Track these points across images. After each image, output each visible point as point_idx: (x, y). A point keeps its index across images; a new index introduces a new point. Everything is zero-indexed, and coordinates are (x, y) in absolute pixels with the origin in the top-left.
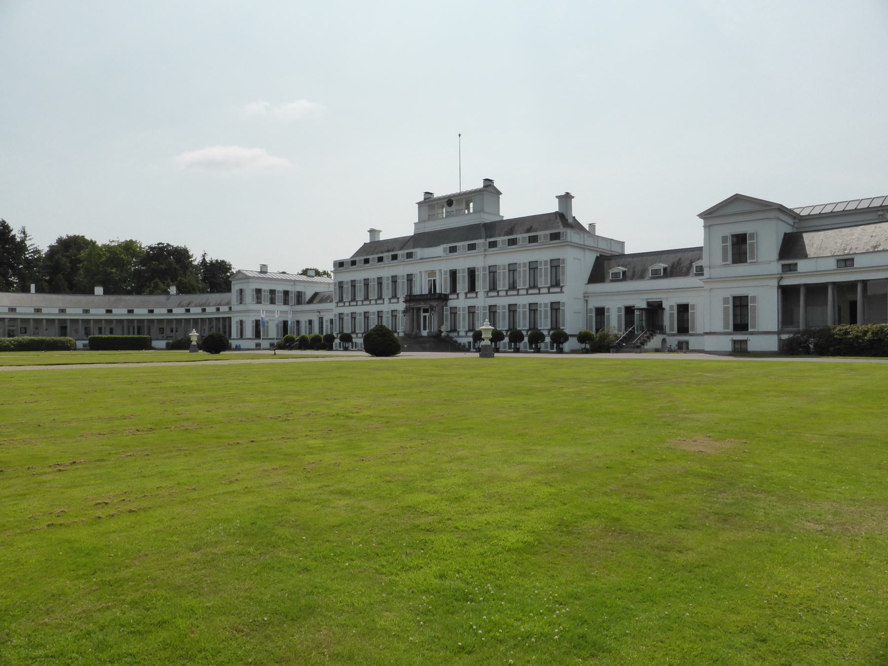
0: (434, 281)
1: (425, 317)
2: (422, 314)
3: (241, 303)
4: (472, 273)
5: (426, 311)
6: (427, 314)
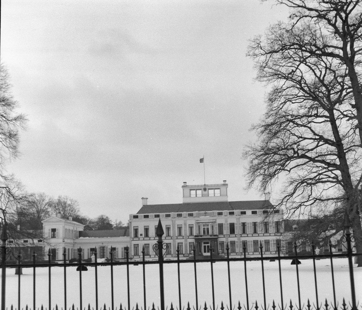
0: (208, 229)
1: (205, 247)
2: (203, 245)
3: (54, 238)
4: (232, 226)
5: (204, 243)
6: (206, 245)
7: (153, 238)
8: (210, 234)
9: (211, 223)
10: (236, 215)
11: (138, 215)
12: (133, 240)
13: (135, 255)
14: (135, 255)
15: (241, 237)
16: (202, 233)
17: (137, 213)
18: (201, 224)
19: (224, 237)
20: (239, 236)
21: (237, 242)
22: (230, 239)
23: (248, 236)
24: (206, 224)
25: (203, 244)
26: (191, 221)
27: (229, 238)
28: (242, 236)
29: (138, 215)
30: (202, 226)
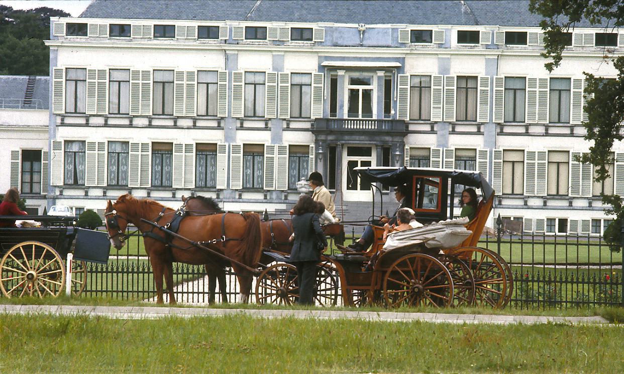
0: (367, 95)
2: (346, 159)
7: (145, 122)
8: (375, 117)
9: (381, 74)
10: (487, 47)
11: (89, 21)
12: (63, 124)
13: (67, 186)
14: (67, 186)
15: (501, 133)
16: (344, 112)
17: (81, 16)
18: (341, 73)
19: (432, 131)
20: (494, 130)
21: (483, 153)
22: (456, 141)
23: (527, 134)
24: (360, 77)
25: (345, 153)
26: (303, 62)
27: (452, 136)
28: (507, 130)
29: (89, 21)
30: (347, 81)
